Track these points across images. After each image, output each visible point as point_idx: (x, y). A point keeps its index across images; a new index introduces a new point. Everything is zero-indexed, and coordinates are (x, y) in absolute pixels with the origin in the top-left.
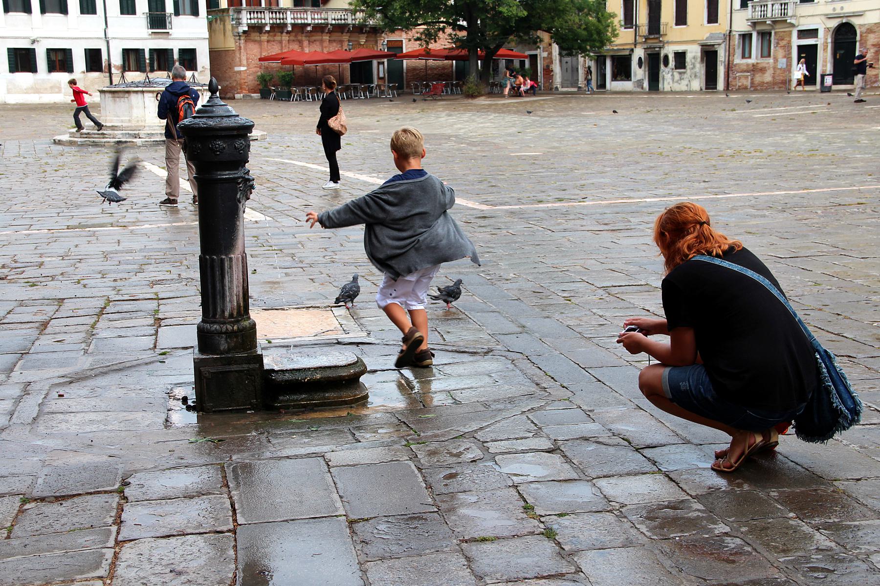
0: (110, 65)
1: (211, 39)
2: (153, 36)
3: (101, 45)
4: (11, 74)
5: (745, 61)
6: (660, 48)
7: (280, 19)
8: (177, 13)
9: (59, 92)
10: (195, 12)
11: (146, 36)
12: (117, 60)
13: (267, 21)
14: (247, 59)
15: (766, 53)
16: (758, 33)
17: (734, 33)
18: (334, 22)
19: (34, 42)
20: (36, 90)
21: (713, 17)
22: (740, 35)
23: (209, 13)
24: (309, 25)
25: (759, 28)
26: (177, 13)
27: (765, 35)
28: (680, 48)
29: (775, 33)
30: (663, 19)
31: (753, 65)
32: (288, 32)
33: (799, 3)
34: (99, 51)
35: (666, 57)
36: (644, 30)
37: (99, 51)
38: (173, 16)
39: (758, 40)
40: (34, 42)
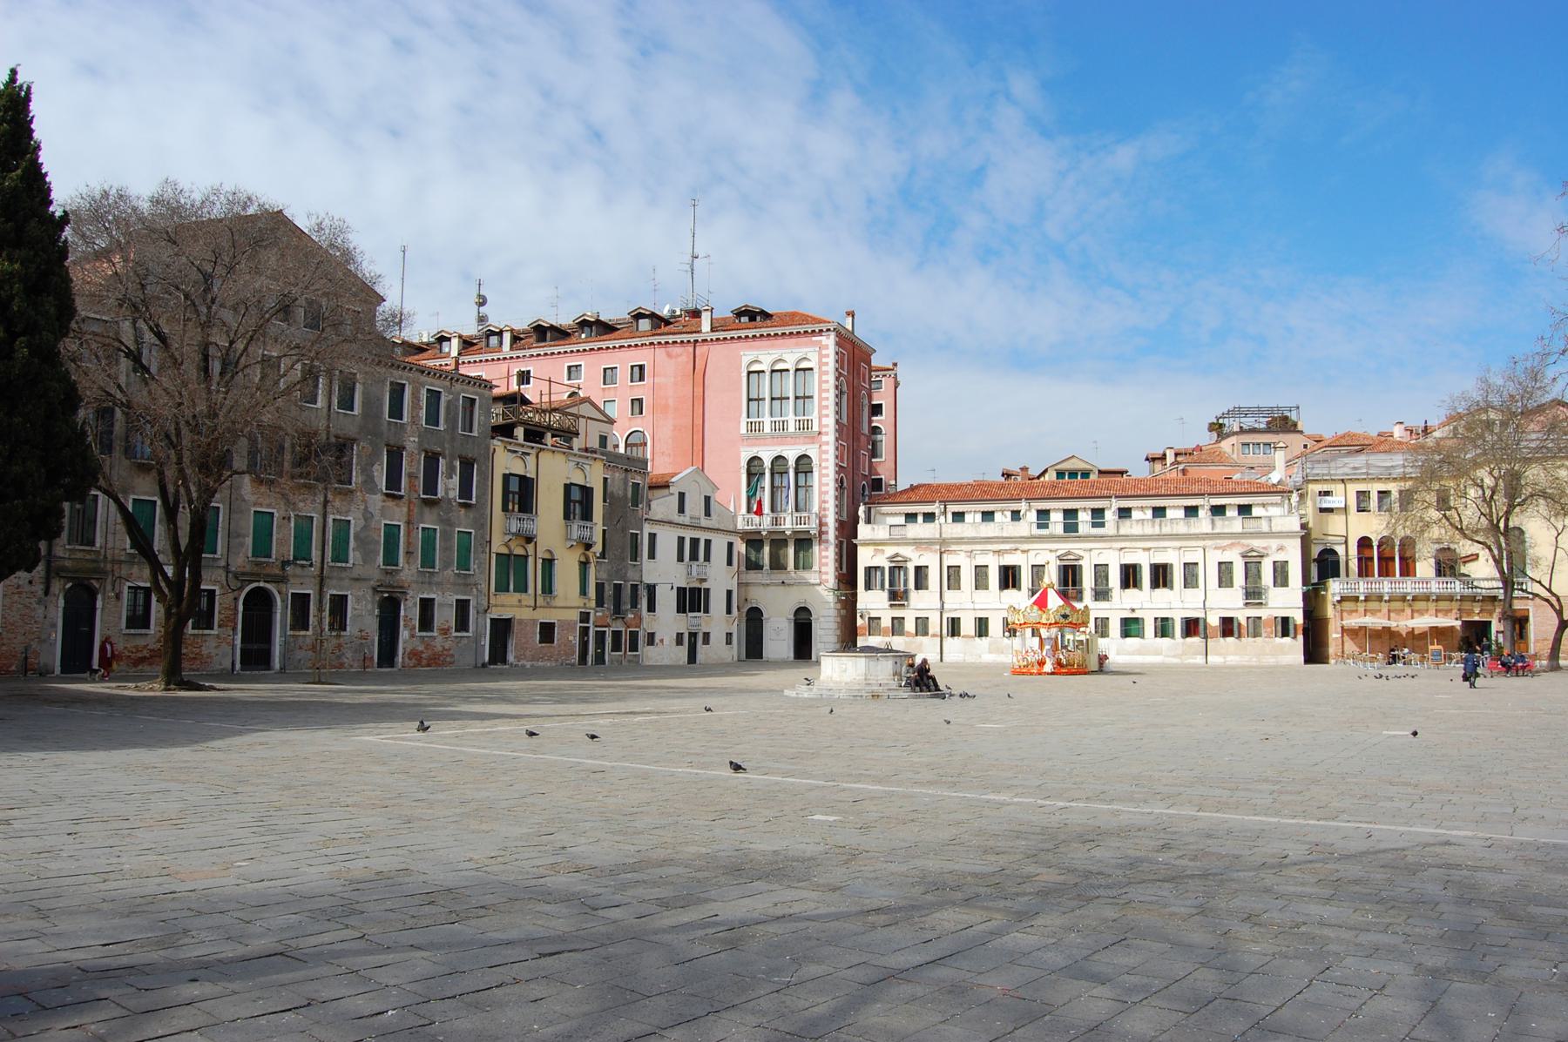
3: (1199, 614)
7: (1347, 589)
9: (1161, 654)
20: (1139, 652)
32: (1386, 601)
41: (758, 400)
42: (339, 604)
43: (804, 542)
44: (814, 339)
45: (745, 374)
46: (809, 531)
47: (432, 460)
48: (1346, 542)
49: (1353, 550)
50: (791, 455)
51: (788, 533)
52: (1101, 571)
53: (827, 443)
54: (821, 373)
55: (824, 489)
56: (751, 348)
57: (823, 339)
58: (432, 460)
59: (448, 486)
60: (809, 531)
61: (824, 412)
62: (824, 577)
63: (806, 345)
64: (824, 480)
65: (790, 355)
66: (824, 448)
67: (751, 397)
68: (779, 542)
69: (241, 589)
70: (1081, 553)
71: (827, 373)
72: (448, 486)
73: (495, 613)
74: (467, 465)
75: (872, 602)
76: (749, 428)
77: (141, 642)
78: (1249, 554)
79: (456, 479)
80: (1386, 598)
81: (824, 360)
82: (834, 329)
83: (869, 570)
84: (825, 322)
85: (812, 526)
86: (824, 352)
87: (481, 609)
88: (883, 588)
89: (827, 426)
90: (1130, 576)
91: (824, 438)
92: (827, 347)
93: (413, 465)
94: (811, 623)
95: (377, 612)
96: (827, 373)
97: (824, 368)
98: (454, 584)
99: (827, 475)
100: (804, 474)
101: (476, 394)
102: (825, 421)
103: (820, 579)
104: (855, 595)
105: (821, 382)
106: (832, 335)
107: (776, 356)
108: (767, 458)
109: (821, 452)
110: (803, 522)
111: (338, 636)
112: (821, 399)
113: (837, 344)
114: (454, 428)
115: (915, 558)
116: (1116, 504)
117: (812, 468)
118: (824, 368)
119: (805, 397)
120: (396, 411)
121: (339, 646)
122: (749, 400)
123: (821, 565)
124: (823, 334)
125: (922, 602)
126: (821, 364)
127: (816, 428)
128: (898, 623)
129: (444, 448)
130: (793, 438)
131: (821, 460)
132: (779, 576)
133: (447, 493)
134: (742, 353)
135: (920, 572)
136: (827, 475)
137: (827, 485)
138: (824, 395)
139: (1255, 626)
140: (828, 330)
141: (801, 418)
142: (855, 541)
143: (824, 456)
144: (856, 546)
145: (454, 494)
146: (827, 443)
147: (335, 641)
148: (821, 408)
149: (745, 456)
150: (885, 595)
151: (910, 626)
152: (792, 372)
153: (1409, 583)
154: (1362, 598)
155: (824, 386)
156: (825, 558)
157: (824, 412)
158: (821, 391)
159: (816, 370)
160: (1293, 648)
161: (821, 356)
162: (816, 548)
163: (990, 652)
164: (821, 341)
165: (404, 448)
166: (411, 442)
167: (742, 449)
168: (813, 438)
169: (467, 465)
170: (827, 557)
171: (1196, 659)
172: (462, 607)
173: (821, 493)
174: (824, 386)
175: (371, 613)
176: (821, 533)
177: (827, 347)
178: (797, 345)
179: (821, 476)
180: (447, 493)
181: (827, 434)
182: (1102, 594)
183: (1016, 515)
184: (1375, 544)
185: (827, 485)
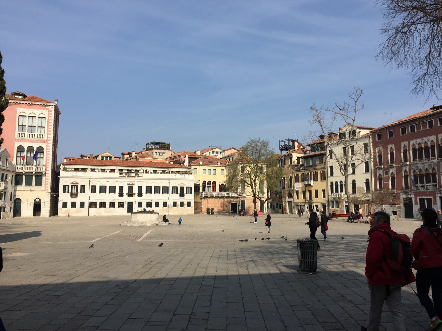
0: (169, 206)
1: (194, 199)
2: (180, 198)
3: (167, 201)
4: (147, 208)
5: (332, 208)
6: (312, 204)
8: (187, 193)
10: (191, 193)
11: (179, 199)
12: (171, 204)
13: (209, 195)
14: (204, 204)
15: (338, 207)
16: (335, 201)
17: (330, 201)
18: (226, 195)
19: (151, 200)
21: (324, 197)
22: (331, 201)
23: (194, 193)
24: (220, 196)
25: (335, 200)
26: (187, 193)
27: (337, 202)
28: (317, 204)
29: (339, 201)
30: (312, 197)
31: (335, 209)
32: (214, 198)
33: (344, 194)
34: (167, 202)
35: (313, 206)
36: (308, 199)
37: (167, 202)
38: (186, 194)
39: (335, 203)
40: (151, 200)
41: (22, 126)
43: (39, 177)
44: (46, 107)
45: (18, 116)
46: (42, 173)
48: (200, 182)
49: (201, 185)
50: (35, 146)
51: (34, 173)
52: (140, 188)
53: (50, 143)
54: (49, 120)
55: (48, 159)
56: (21, 107)
57: (50, 108)
60: (42, 173)
61: (49, 133)
62: (46, 188)
63: (43, 109)
64: (48, 156)
65: (37, 112)
66: (49, 145)
67: (19, 125)
68: (29, 176)
70: (134, 182)
71: (51, 120)
75: (63, 197)
76: (19, 135)
78: (181, 185)
80: (220, 197)
81: (50, 115)
82: (55, 105)
83: (65, 187)
84: (51, 103)
85: (43, 171)
86: (50, 113)
88: (68, 192)
89: (50, 137)
90: (149, 190)
91: (49, 142)
92: (51, 111)
94: (41, 204)
96: (51, 120)
97: (50, 118)
99: (49, 154)
100: (39, 153)
102: (49, 136)
103: (45, 189)
104: (58, 196)
105: (48, 123)
106: (54, 107)
107: (31, 111)
108: (26, 146)
109: (47, 146)
110: (40, 169)
112: (48, 128)
113: (55, 110)
115: (80, 183)
116: (145, 169)
117: (43, 151)
118: (50, 118)
119: (41, 127)
122: (19, 125)
123: (45, 184)
124: (50, 106)
125: (81, 197)
126: (49, 116)
127: (46, 138)
128: (74, 205)
130: (37, 142)
131: (47, 149)
132: (29, 188)
134: (17, 108)
135: (83, 187)
136: (49, 154)
137: (49, 157)
138: (49, 127)
139: (182, 204)
140: (52, 105)
141: (40, 134)
142: (59, 177)
143: (48, 148)
144: (59, 178)
146: (50, 143)
148: (48, 131)
149: (17, 144)
150: (70, 194)
151: (78, 205)
152: (37, 118)
153: (220, 193)
154: (209, 197)
155: (50, 124)
156: (47, 180)
157: (49, 133)
158: (48, 125)
159: (47, 118)
160: (191, 210)
161: (49, 114)
162: (44, 178)
163: (105, 213)
164: (49, 109)
167: (15, 142)
168: (44, 141)
170: (48, 182)
171: (166, 213)
173: (46, 160)
174: (50, 124)
176: (45, 174)
177: (51, 111)
178: (40, 109)
179: (47, 154)
181: (50, 140)
182: (140, 195)
183: (113, 171)
184: (212, 183)
185: (49, 157)
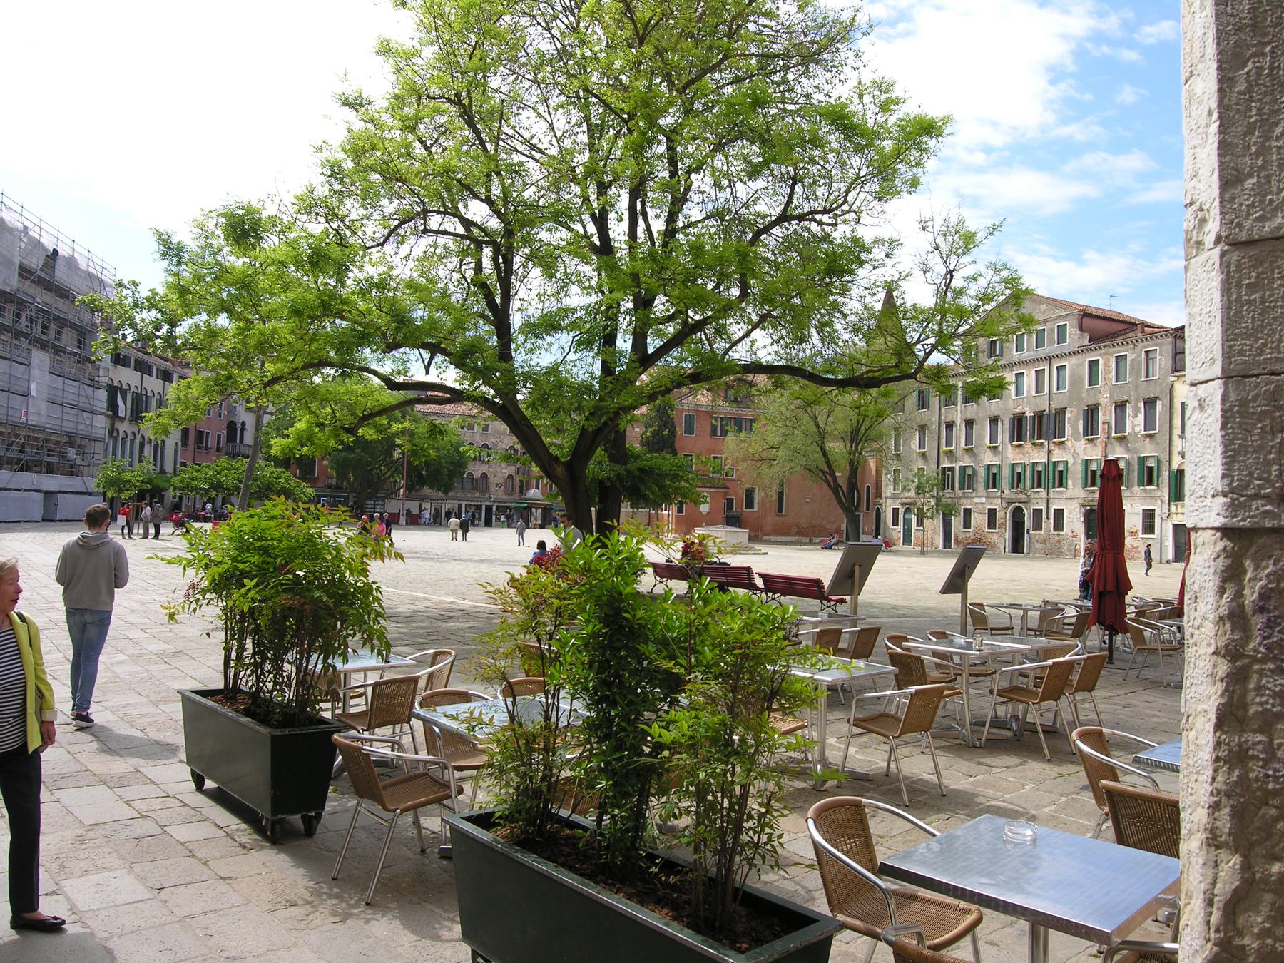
42: (1059, 513)
47: (1121, 406)
58: (1121, 406)
59: (1135, 423)
69: (1008, 507)
72: (1135, 423)
73: (1177, 519)
74: (1150, 403)
77: (968, 535)
79: (1141, 417)
87: (1165, 517)
93: (1106, 415)
95: (1082, 519)
98: (1141, 498)
101: (1157, 345)
111: (1058, 535)
114: (1139, 375)
120: (1093, 379)
121: (1059, 542)
129: (1130, 396)
133: (1133, 429)
145: (1140, 428)
147: (1057, 538)
165: (1099, 404)
166: (1105, 400)
169: (1150, 403)
172: (1149, 516)
175: (1078, 520)
180: (1133, 429)
